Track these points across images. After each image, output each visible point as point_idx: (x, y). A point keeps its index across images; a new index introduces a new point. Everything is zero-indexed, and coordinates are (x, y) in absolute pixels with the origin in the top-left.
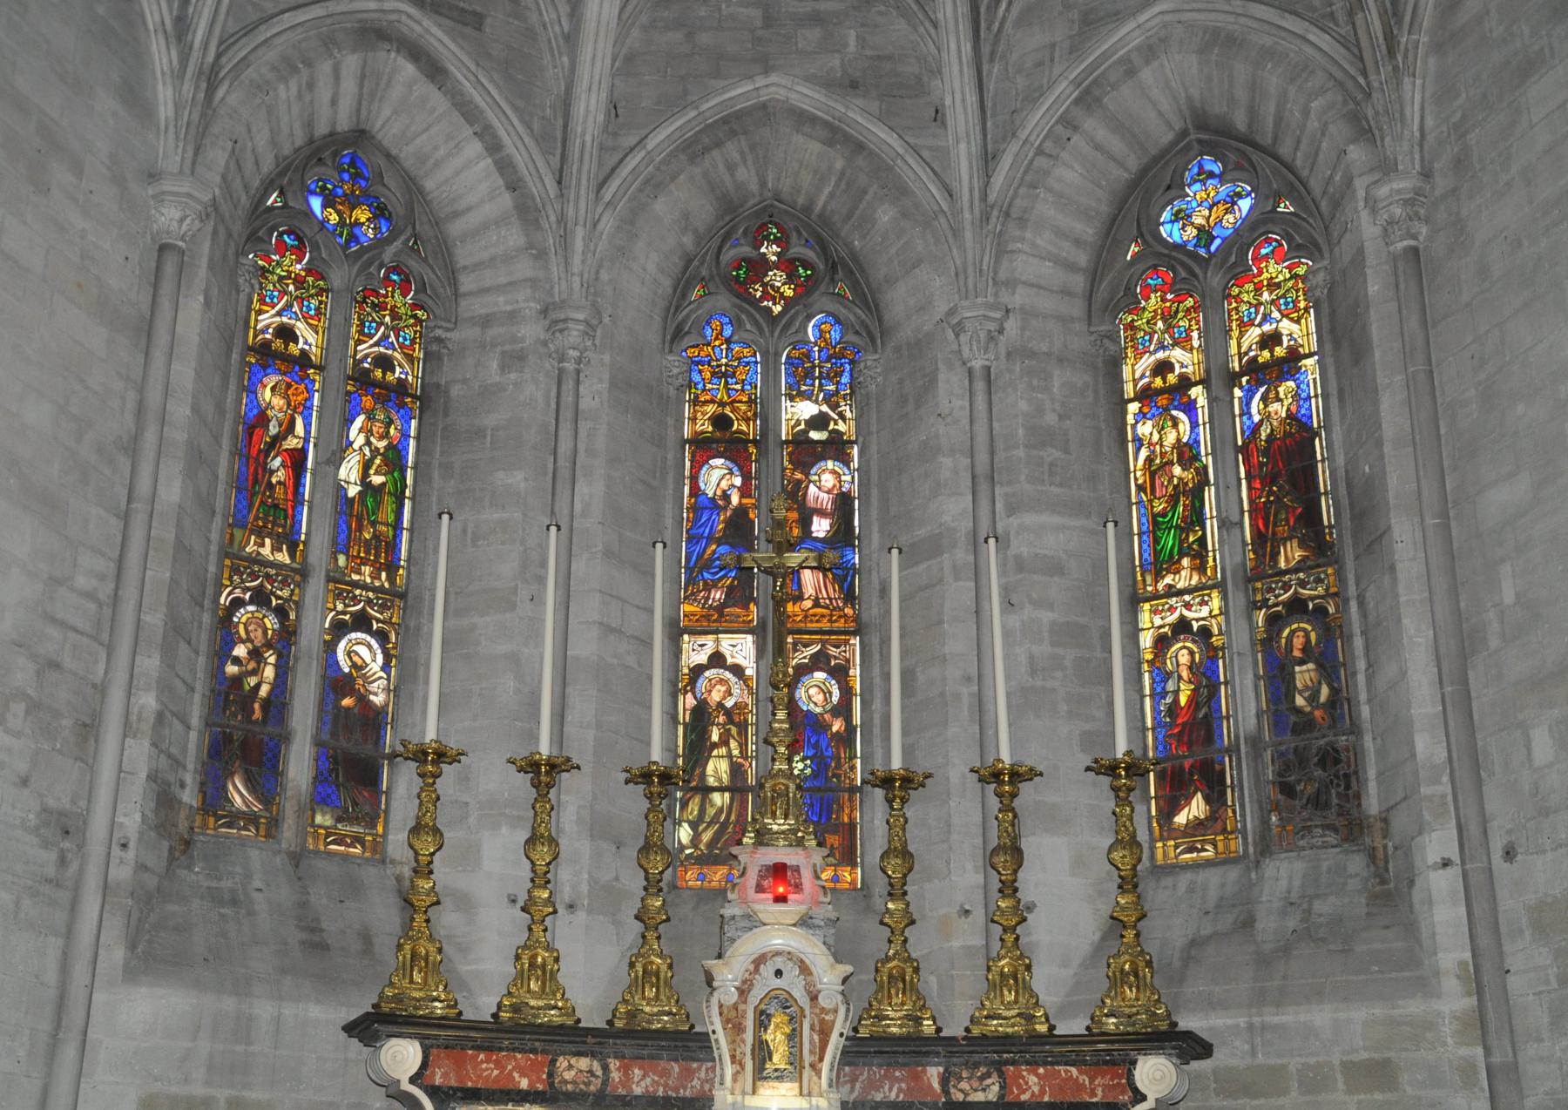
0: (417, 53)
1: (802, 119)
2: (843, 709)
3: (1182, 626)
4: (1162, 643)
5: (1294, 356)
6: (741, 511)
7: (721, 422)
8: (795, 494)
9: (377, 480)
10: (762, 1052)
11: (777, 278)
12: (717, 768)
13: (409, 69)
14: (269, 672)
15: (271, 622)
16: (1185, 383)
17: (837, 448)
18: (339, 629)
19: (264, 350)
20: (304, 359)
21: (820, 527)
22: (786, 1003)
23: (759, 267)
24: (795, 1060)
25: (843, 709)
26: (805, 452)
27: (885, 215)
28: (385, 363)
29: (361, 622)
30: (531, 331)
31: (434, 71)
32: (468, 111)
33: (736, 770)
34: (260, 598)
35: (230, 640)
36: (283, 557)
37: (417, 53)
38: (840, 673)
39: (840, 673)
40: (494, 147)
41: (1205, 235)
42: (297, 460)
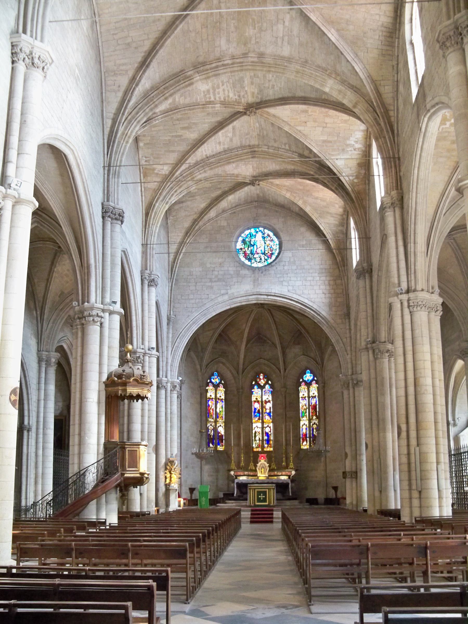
0: (222, 363)
1: (265, 364)
2: (270, 431)
3: (304, 424)
4: (303, 426)
5: (316, 396)
6: (259, 410)
7: (257, 399)
8: (265, 407)
9: (221, 410)
10: (261, 472)
11: (262, 381)
12: (257, 438)
13: (221, 365)
14: (213, 433)
15: (212, 427)
16: (305, 397)
17: (269, 401)
18: (218, 427)
19: (209, 398)
20: (213, 398)
21: (268, 411)
22: (263, 467)
23: (260, 379)
24: (264, 472)
25: (270, 431)
26: (266, 402)
27: (274, 376)
28: (220, 396)
29: (220, 426)
30: (236, 392)
31: (224, 364)
32: (228, 368)
33: (259, 438)
34: (211, 425)
35: (209, 430)
36: (213, 420)
37: (222, 363)
38: (270, 427)
39: (270, 427)
40: (231, 371)
41: (308, 380)
42: (213, 409)
